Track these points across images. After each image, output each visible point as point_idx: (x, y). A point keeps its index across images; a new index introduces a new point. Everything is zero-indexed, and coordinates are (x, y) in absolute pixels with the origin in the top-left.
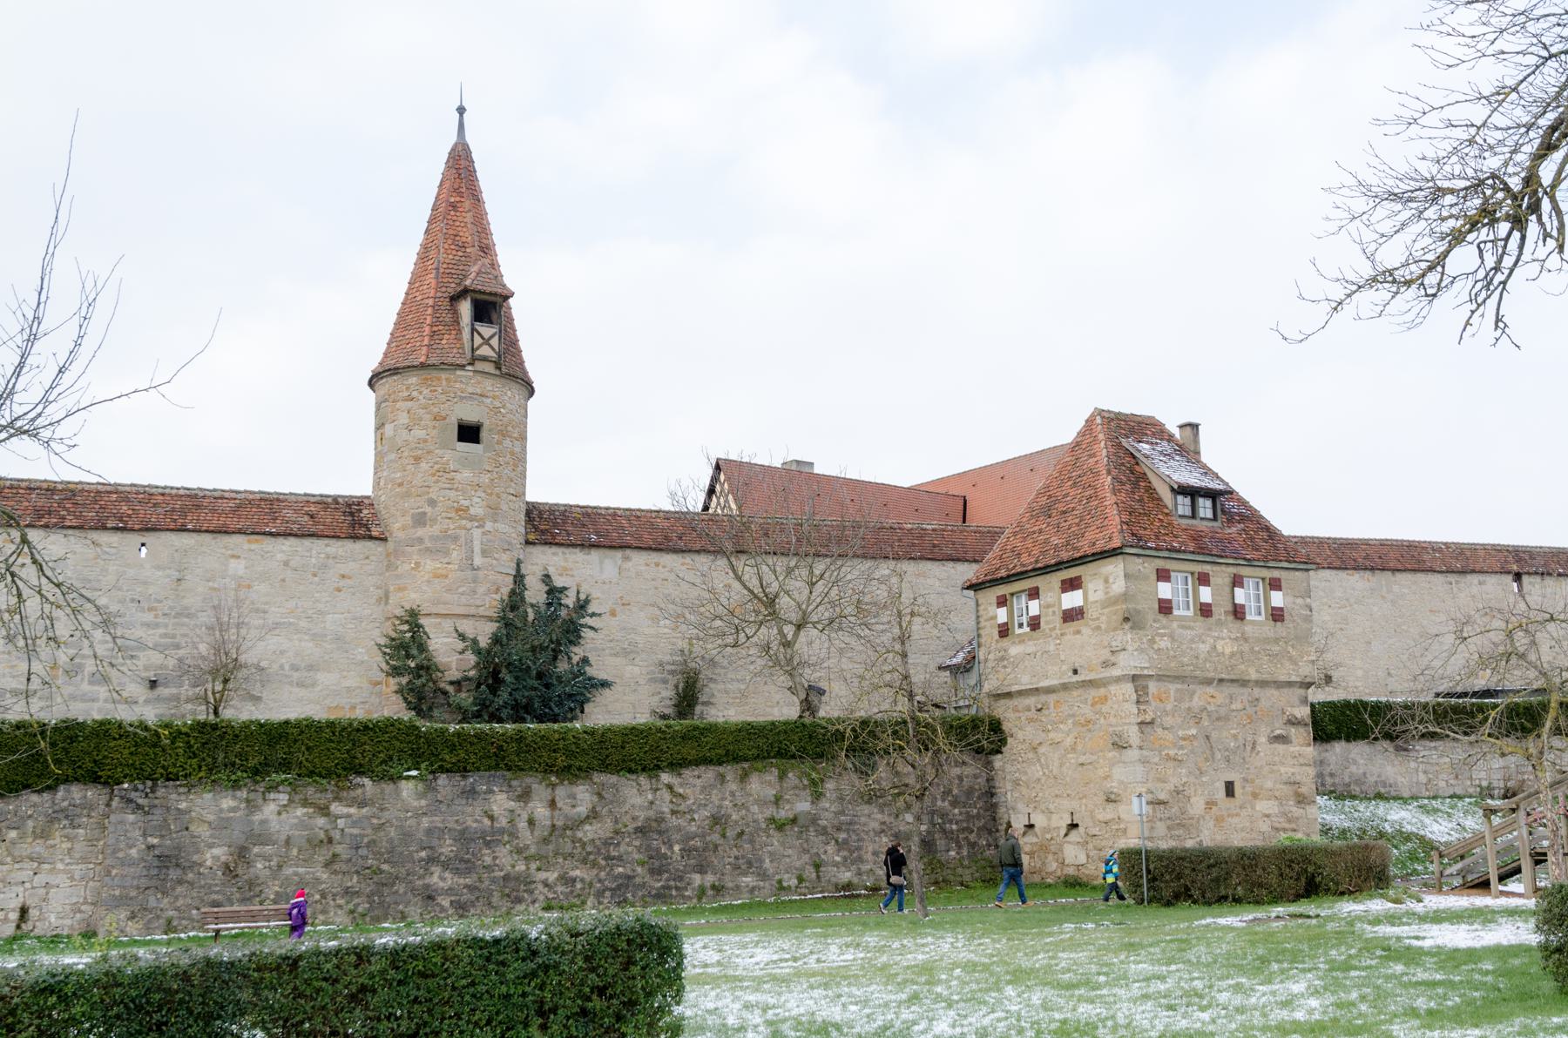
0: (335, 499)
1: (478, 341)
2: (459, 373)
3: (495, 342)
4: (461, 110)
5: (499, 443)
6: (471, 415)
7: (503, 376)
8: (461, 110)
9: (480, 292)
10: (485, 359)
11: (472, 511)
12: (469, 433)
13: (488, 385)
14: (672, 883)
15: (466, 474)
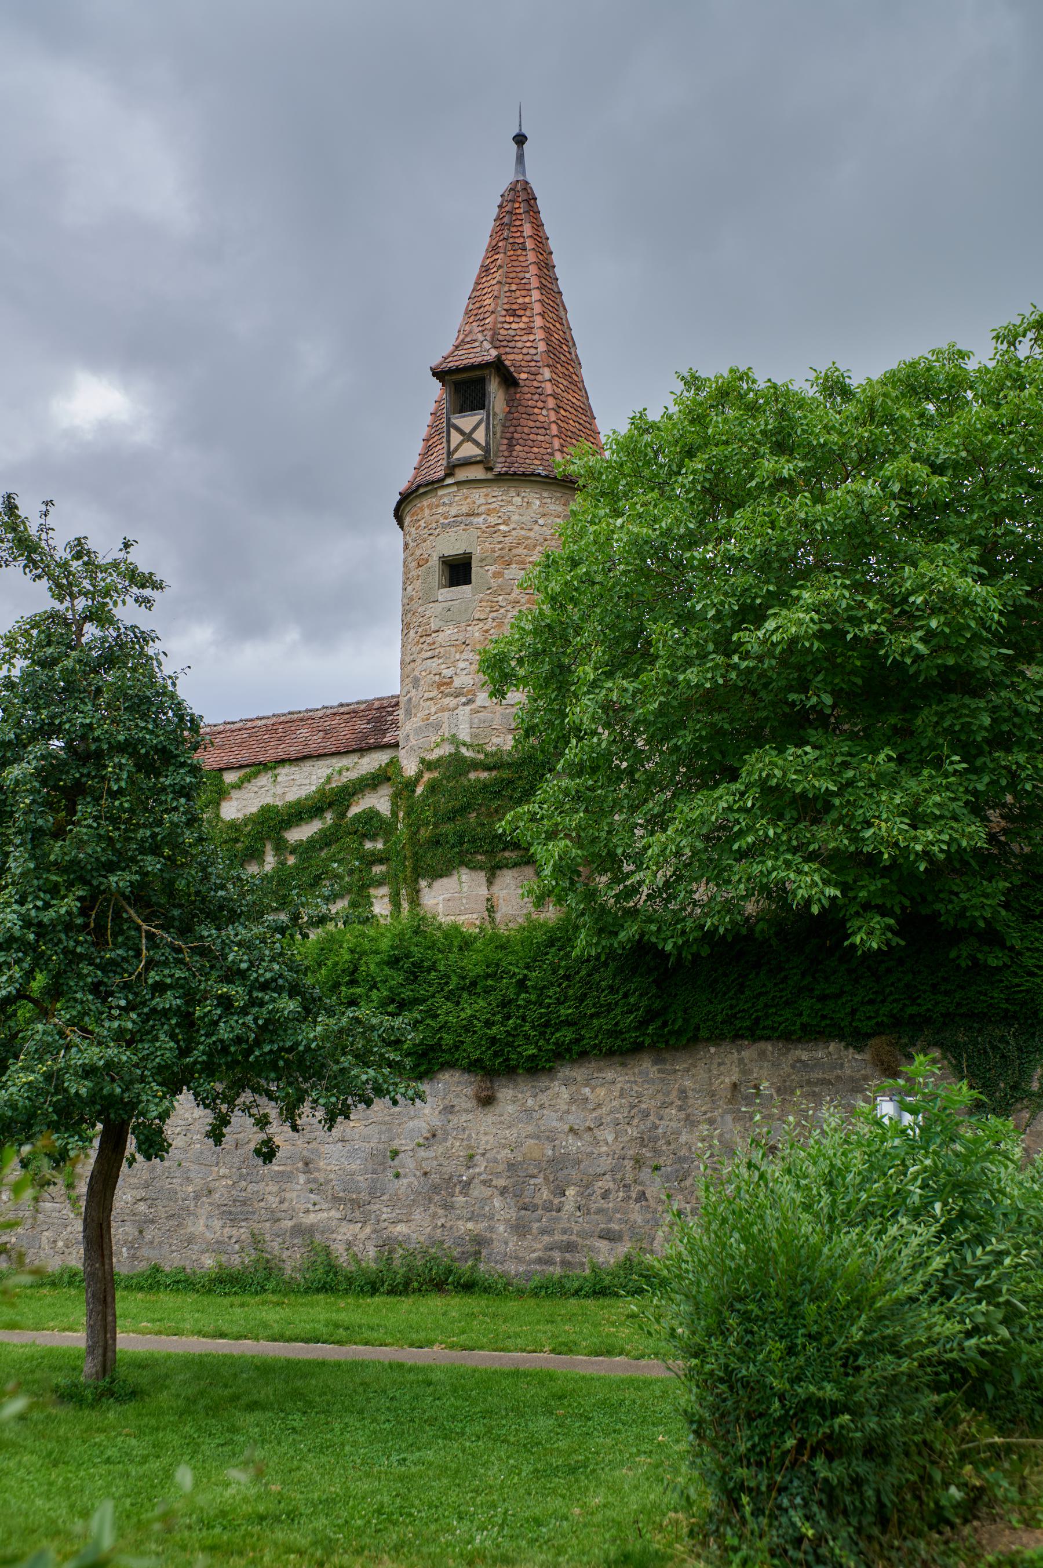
0: (369, 703)
1: (456, 438)
2: (440, 492)
3: (480, 435)
4: (520, 140)
5: (497, 575)
6: (452, 544)
7: (502, 478)
8: (520, 140)
9: (458, 370)
10: (467, 463)
11: (457, 682)
12: (458, 571)
13: (478, 496)
14: (557, 1256)
15: (450, 631)
